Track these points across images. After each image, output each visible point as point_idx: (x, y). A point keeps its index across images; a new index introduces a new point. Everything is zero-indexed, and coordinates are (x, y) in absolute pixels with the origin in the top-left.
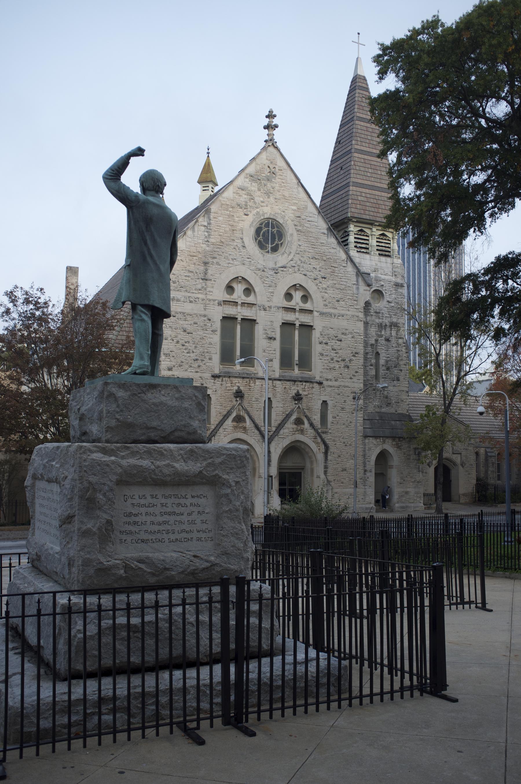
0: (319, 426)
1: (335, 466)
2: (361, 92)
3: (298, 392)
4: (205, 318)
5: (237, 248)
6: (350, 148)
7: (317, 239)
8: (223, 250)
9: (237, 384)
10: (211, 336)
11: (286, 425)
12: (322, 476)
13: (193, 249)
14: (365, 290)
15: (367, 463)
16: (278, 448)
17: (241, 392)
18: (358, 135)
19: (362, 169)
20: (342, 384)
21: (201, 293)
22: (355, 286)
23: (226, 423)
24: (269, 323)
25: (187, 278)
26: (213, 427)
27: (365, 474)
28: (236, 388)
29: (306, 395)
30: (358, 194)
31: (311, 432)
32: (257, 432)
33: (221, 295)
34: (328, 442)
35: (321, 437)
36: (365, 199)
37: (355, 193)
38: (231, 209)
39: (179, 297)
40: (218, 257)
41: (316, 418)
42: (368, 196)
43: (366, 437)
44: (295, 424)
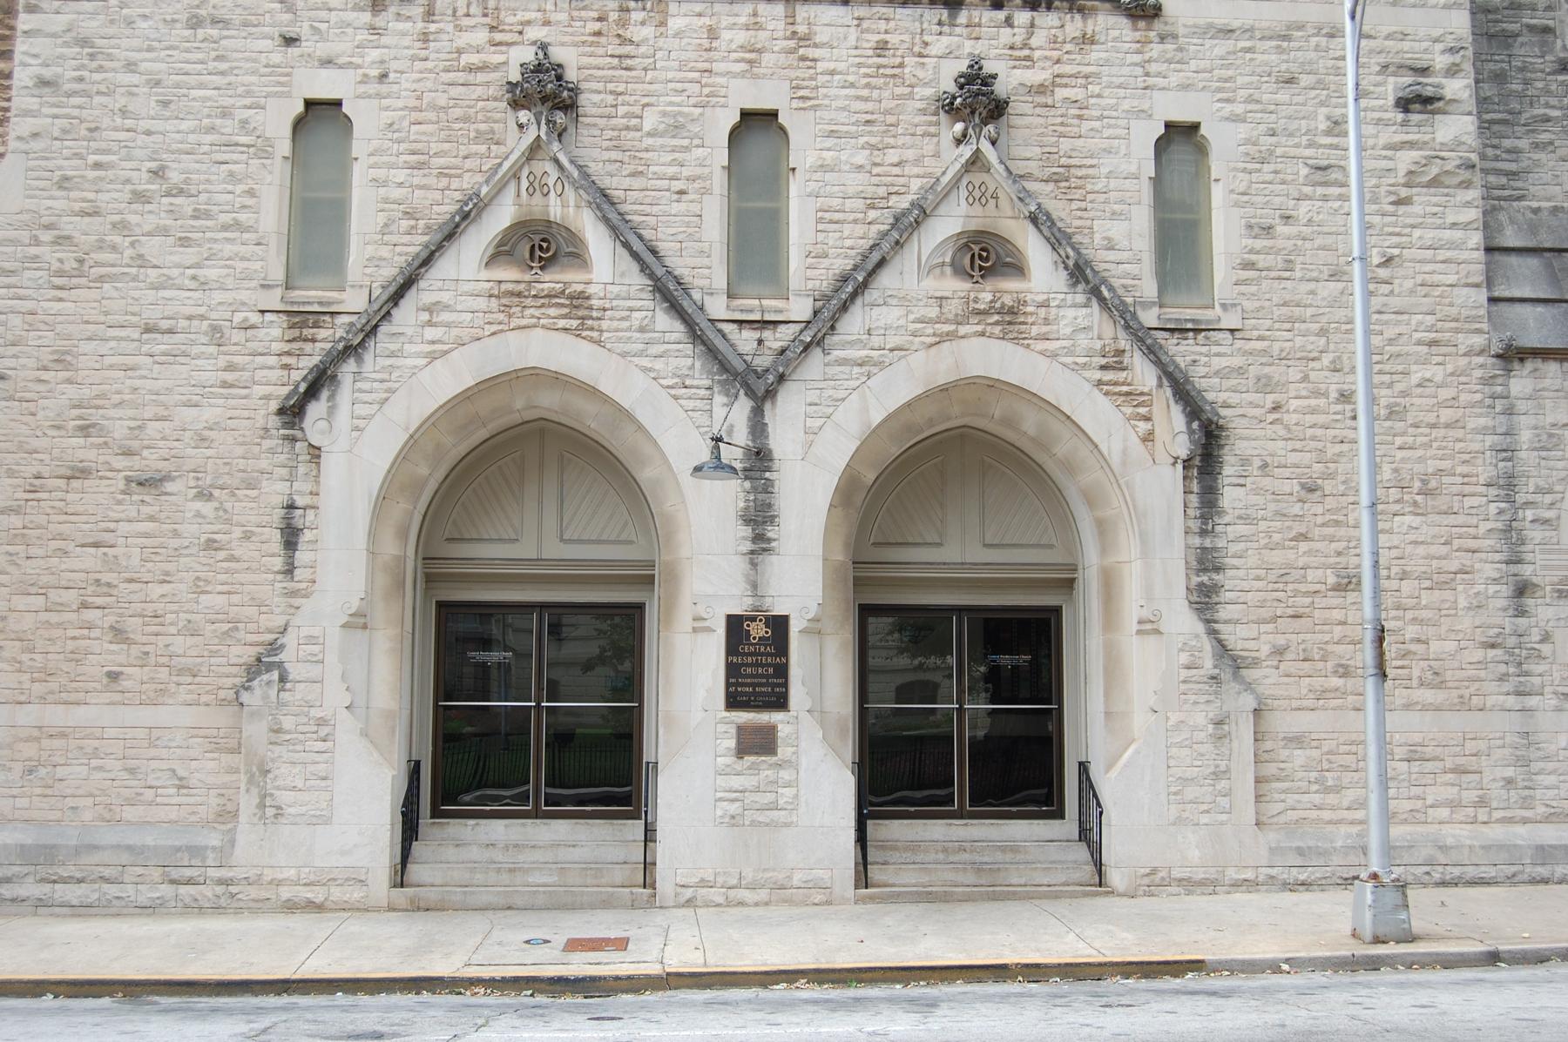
0: (1149, 289)
1: (1277, 557)
3: (976, 64)
9: (534, 33)
11: (886, 279)
12: (1182, 622)
15: (1535, 534)
16: (824, 435)
17: (558, 71)
23: (444, 267)
26: (355, 301)
27: (1521, 612)
28: (528, 55)
29: (1041, 89)
31: (1080, 323)
32: (665, 321)
34: (1214, 392)
35: (1153, 353)
41: (1124, 239)
43: (1513, 355)
44: (959, 271)
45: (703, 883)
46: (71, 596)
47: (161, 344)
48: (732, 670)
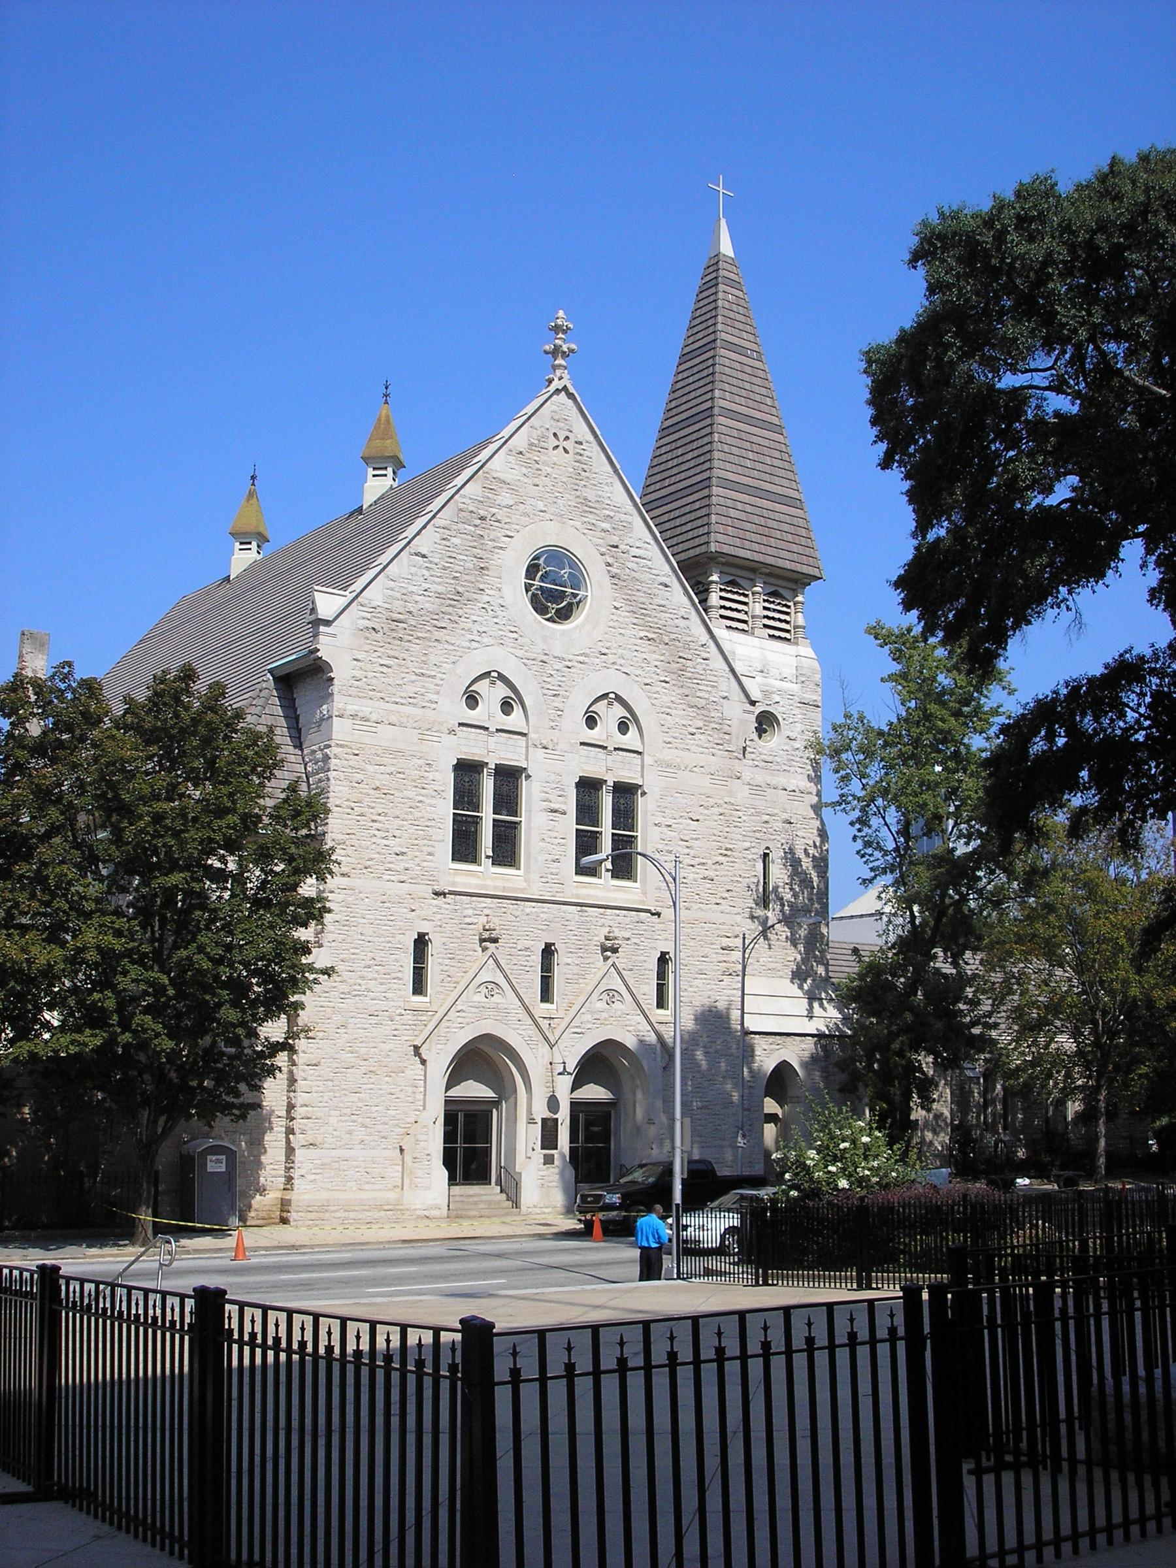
2: (728, 289)
4: (421, 762)
5: (489, 609)
6: (709, 404)
8: (460, 612)
10: (433, 801)
13: (398, 605)
18: (724, 378)
19: (735, 450)
20: (701, 914)
21: (414, 705)
24: (553, 777)
25: (385, 669)
30: (729, 503)
33: (455, 709)
36: (743, 516)
37: (722, 501)
42: (749, 509)
45: (535, 1207)
46: (348, 1111)
47: (374, 1020)
48: (543, 1136)
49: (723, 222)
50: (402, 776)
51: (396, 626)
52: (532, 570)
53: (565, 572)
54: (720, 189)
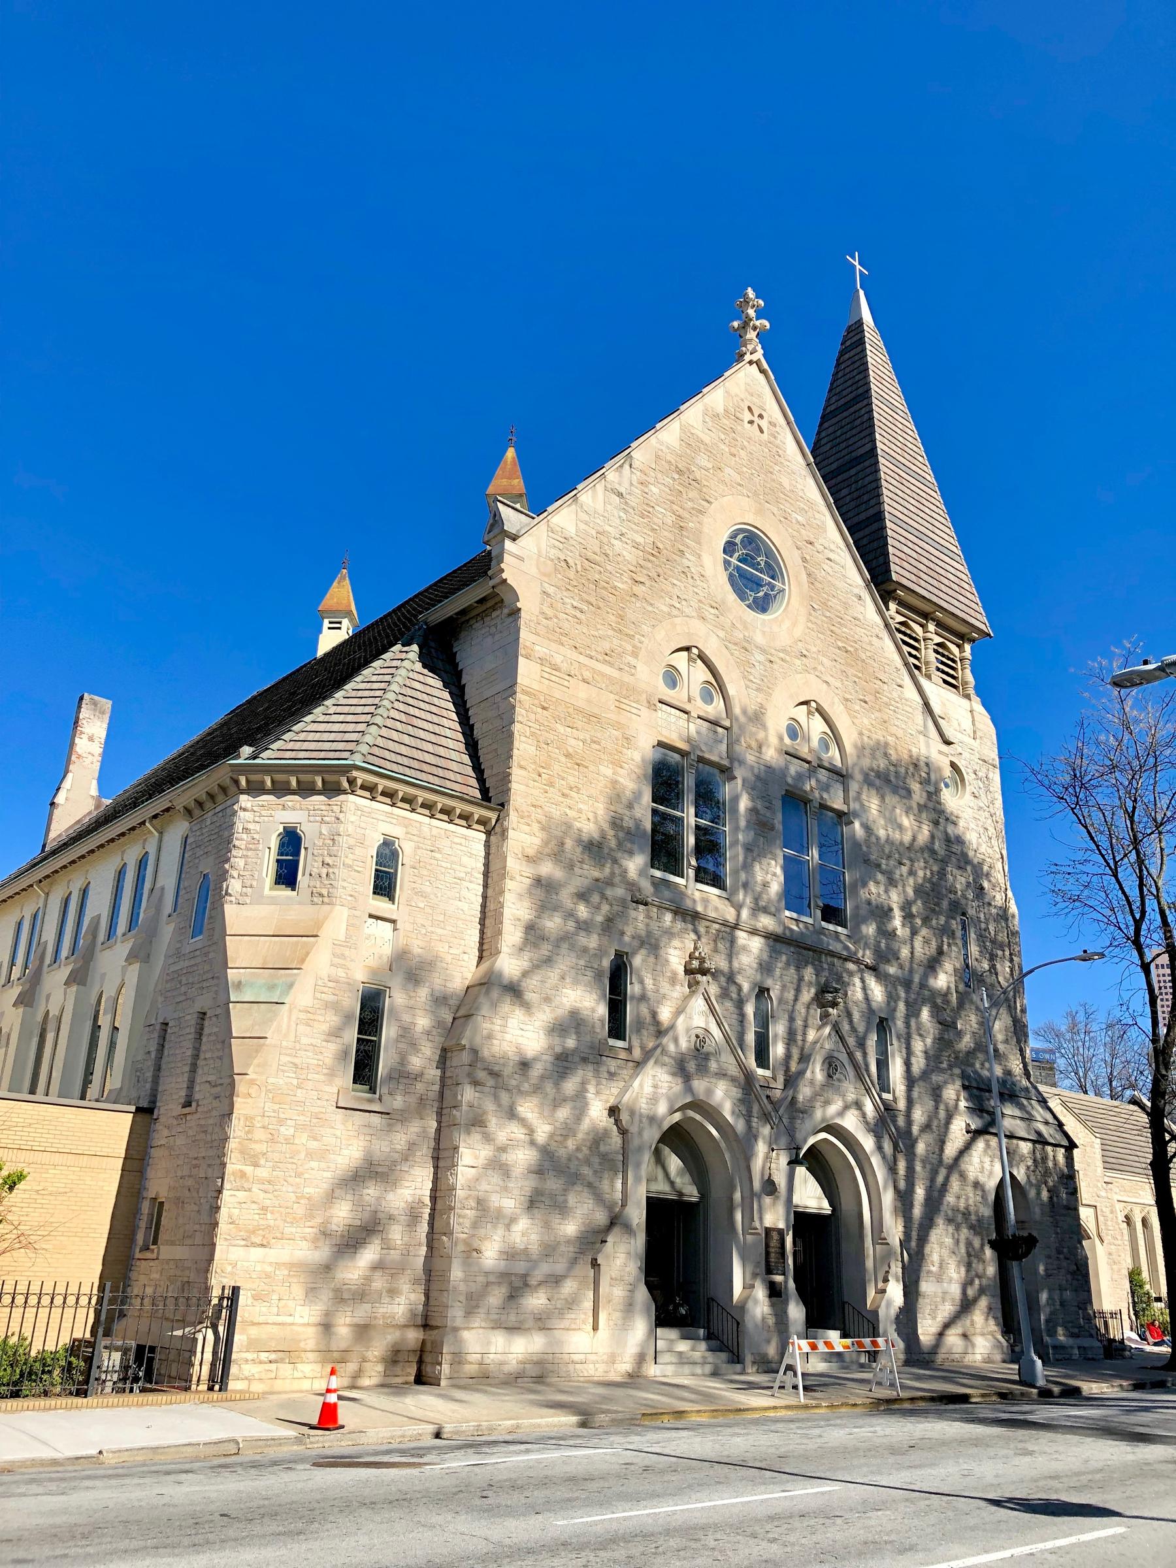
7: (846, 606)
8: (659, 570)
14: (940, 752)
21: (611, 665)
22: (921, 737)
25: (578, 614)
38: (676, 476)
39: (558, 659)
40: (648, 583)
49: (862, 293)
50: (598, 747)
51: (584, 573)
52: (729, 548)
53: (761, 560)
54: (856, 263)
